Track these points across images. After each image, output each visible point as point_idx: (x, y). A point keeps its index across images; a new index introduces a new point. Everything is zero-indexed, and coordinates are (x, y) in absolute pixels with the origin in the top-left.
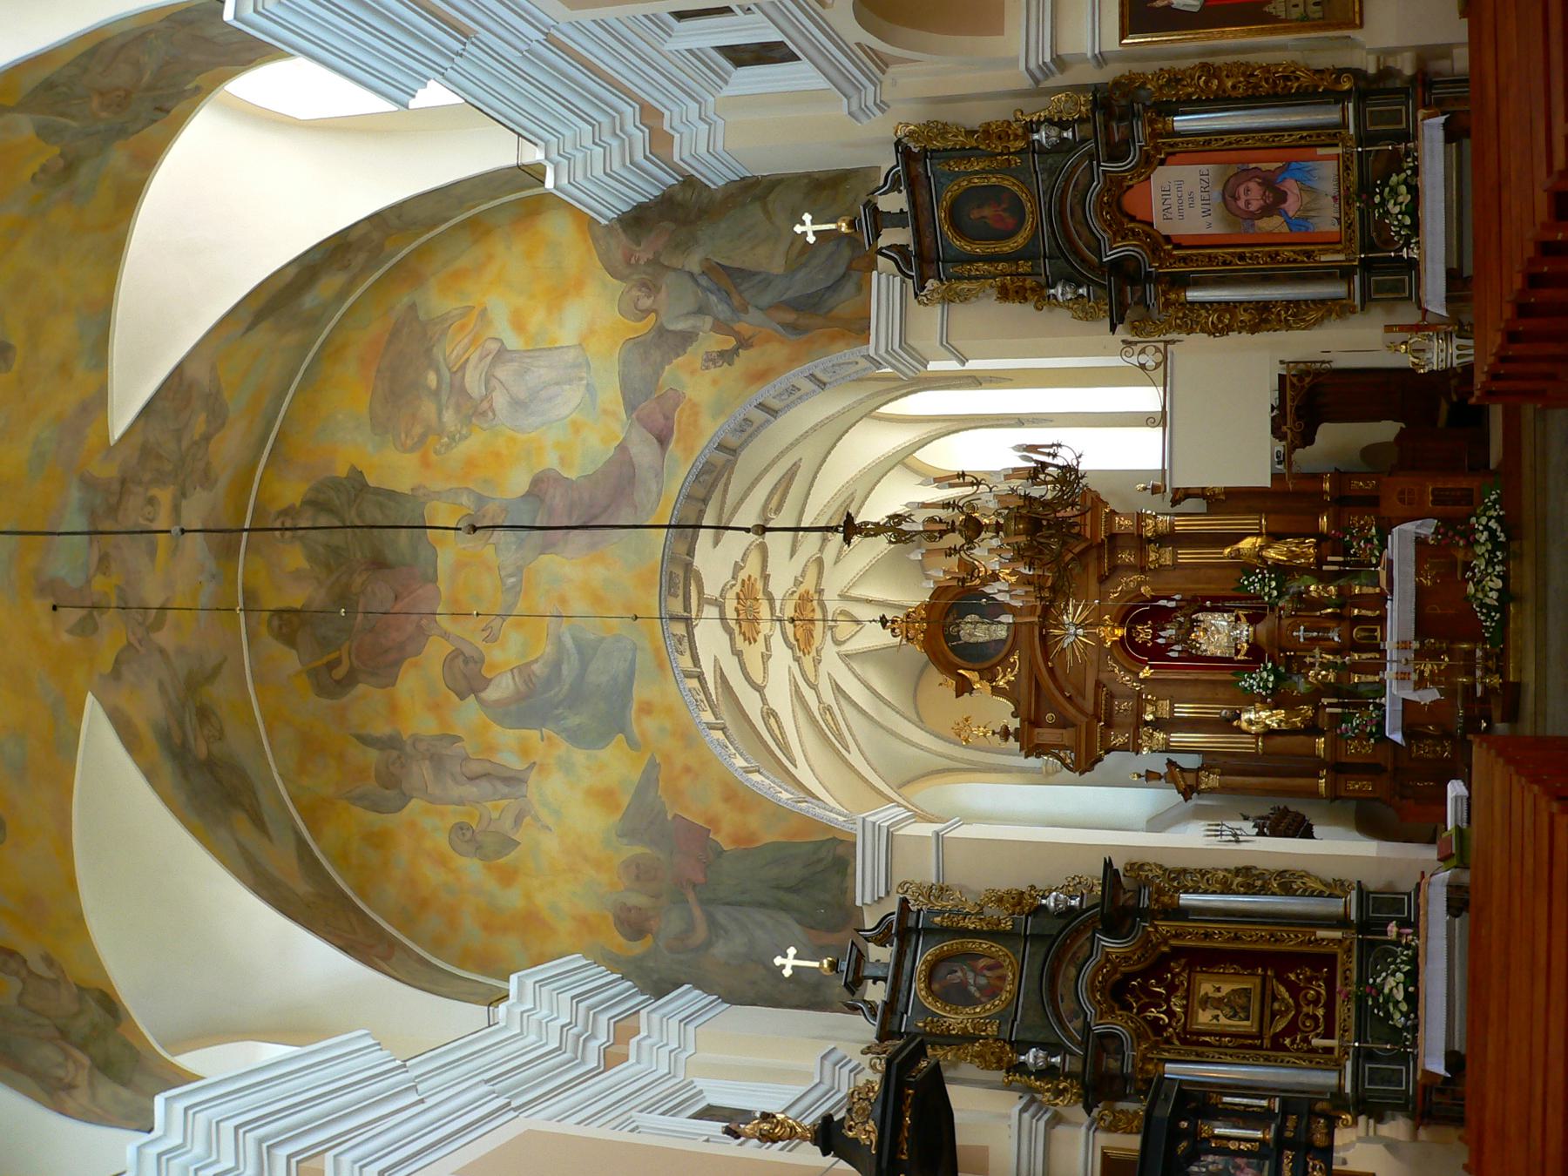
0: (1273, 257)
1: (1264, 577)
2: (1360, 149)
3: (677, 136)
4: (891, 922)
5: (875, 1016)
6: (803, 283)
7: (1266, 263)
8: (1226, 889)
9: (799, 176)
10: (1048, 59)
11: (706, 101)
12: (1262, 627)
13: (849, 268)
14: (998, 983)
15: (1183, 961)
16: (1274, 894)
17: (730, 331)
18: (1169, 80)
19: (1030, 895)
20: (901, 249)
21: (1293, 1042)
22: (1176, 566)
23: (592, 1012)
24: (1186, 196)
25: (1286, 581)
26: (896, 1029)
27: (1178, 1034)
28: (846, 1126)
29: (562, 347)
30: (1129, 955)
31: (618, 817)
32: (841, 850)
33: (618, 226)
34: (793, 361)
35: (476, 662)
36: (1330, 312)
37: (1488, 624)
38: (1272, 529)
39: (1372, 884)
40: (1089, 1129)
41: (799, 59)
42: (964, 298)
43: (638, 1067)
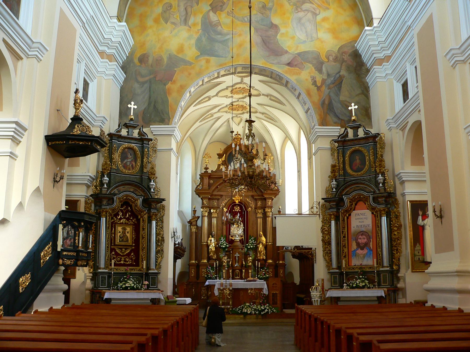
0: (344, 246)
1: (254, 244)
2: (376, 272)
3: (381, 67)
4: (145, 136)
5: (117, 132)
6: (337, 106)
7: (342, 244)
8: (157, 234)
10: (403, 179)
11: (392, 76)
12: (239, 243)
13: (342, 120)
14: (128, 169)
15: (136, 222)
16: (156, 248)
18: (397, 215)
19: (154, 177)
20: (347, 135)
21: (113, 254)
22: (257, 218)
23: (116, 48)
24: (362, 220)
25: (253, 250)
26: (113, 138)
27: (114, 221)
28: (79, 125)
29: (317, 33)
30: (137, 207)
31: (175, 53)
32: (166, 120)
33: (354, 49)
34: (313, 103)
35: (221, 9)
36: (328, 263)
37: (237, 309)
39: (160, 277)
40: (86, 196)
41: (404, 103)
42: (332, 155)
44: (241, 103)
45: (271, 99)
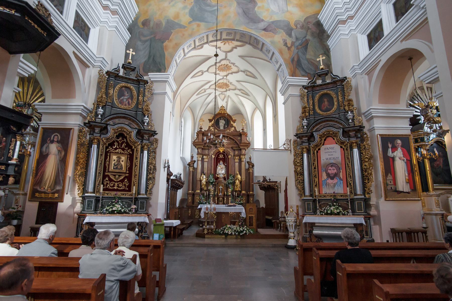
1: (232, 180)
2: (349, 199)
9: (330, 62)
10: (373, 115)
11: (355, 31)
12: (222, 179)
13: (308, 73)
15: (131, 152)
17: (292, 46)
21: (107, 180)
22: (235, 162)
23: (118, 4)
24: (332, 153)
27: (110, 150)
31: (172, 19)
32: (163, 70)
34: (285, 60)
37: (220, 230)
38: (242, 181)
39: (151, 202)
41: (370, 51)
43: (102, 13)
44: (225, 81)
45: (247, 75)
